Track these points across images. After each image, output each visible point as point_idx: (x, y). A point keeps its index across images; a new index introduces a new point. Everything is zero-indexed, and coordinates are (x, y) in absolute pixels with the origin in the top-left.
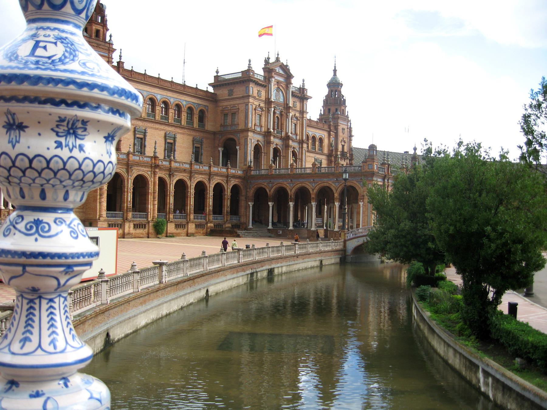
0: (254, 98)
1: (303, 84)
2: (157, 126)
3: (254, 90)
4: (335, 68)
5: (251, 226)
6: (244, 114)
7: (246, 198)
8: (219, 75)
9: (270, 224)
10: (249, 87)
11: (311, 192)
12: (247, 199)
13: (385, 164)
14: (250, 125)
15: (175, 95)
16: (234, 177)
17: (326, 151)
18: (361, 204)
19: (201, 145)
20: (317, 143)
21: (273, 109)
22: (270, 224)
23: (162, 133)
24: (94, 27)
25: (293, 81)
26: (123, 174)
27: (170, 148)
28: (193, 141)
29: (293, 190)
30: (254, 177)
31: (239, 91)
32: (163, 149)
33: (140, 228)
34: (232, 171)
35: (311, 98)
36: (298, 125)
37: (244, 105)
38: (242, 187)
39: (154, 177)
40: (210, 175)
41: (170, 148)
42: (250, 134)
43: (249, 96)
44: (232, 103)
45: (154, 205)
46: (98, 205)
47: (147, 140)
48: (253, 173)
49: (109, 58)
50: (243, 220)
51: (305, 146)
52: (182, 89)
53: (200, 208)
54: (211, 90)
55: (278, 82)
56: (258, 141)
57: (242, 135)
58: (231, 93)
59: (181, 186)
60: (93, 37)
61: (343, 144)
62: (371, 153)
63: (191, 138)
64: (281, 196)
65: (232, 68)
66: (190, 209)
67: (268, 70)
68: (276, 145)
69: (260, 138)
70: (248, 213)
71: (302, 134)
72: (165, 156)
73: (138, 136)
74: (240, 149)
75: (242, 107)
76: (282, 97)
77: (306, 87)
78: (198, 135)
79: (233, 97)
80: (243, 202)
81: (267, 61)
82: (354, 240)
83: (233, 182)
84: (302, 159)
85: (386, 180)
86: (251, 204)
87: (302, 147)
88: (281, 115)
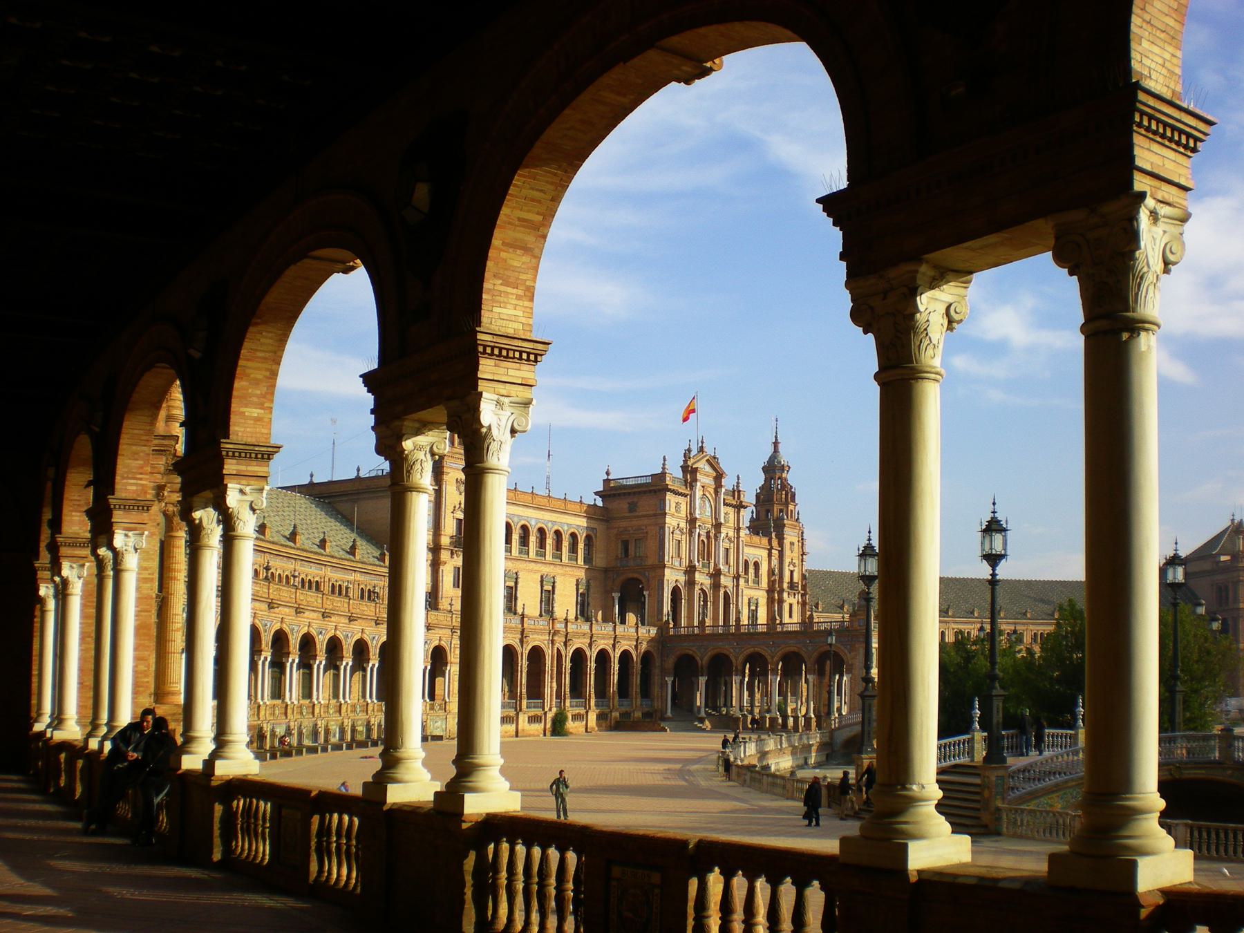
2: (532, 566)
5: (669, 714)
12: (664, 673)
27: (548, 599)
28: (577, 585)
41: (548, 599)
44: (635, 522)
50: (657, 704)
53: (601, 692)
54: (600, 503)
58: (632, 508)
59: (579, 656)
65: (633, 467)
76: (708, 509)
86: (669, 680)
87: (738, 586)
88: (708, 537)
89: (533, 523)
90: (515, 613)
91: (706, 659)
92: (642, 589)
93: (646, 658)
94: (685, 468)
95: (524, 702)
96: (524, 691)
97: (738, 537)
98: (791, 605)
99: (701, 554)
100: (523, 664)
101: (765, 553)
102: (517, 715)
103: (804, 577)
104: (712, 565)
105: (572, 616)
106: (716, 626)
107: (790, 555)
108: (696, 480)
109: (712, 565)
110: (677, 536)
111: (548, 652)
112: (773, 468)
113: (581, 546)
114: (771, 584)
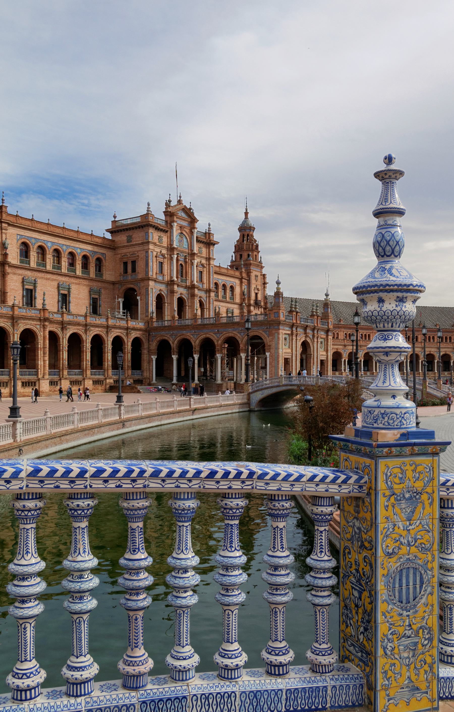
0: (155, 244)
2: (49, 276)
3: (154, 236)
4: (246, 211)
5: (154, 381)
6: (145, 262)
7: (149, 352)
8: (116, 219)
10: (148, 232)
11: (216, 343)
13: (293, 311)
14: (150, 273)
15: (68, 243)
17: (238, 299)
18: (268, 354)
19: (99, 296)
20: (228, 291)
21: (176, 256)
23: (55, 284)
25: (197, 225)
26: (8, 328)
27: (64, 299)
28: (90, 292)
29: (197, 342)
30: (156, 329)
31: (138, 236)
33: (29, 385)
34: (132, 324)
35: (218, 243)
36: (205, 272)
37: (144, 252)
38: (144, 340)
39: (44, 331)
40: (108, 328)
41: (64, 299)
42: (151, 283)
43: (148, 242)
44: (131, 250)
45: (44, 361)
47: (37, 291)
48: (155, 324)
51: (212, 294)
52: (76, 236)
54: (108, 236)
55: (181, 227)
56: (160, 290)
57: (142, 284)
58: (129, 239)
59: (75, 340)
61: (257, 292)
62: (277, 301)
64: (185, 348)
65: (129, 212)
66: (86, 364)
67: (169, 214)
68: (181, 294)
69: (163, 287)
70: (151, 368)
71: (209, 282)
73: (26, 287)
74: (141, 300)
75: (142, 255)
77: (212, 232)
78: (96, 285)
79: (132, 243)
80: (145, 356)
81: (168, 204)
82: (258, 393)
83: (134, 335)
84: (209, 309)
85: (294, 329)
86: (154, 358)
87: (209, 296)
88: (186, 262)
89: (49, 244)
91: (176, 342)
92: (136, 295)
101: (237, 282)
114: (243, 300)
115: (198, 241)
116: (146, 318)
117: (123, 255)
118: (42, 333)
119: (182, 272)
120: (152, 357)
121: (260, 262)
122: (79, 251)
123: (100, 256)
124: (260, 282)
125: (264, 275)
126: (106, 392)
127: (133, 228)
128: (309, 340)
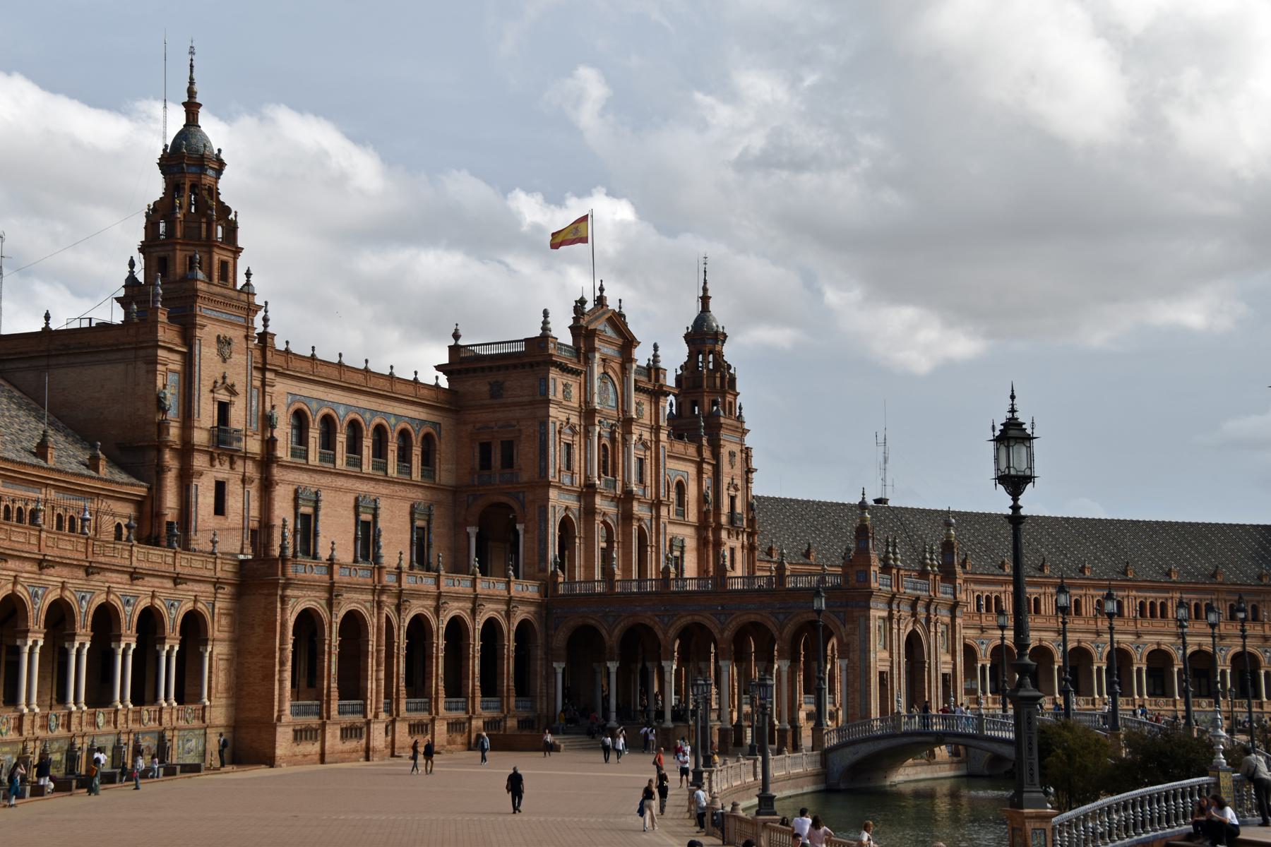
1: (655, 356)
2: (340, 482)
8: (461, 342)
9: (613, 715)
10: (546, 380)
12: (550, 656)
14: (551, 471)
16: (523, 601)
17: (692, 516)
22: (613, 715)
23: (350, 499)
24: (216, 258)
28: (412, 514)
32: (352, 536)
36: (648, 461)
38: (536, 625)
39: (379, 613)
42: (553, 494)
45: (378, 680)
46: (277, 687)
47: (321, 518)
49: (248, 328)
51: (664, 511)
54: (444, 382)
55: (604, 360)
56: (567, 508)
58: (497, 391)
60: (216, 281)
61: (732, 493)
63: (407, 507)
71: (657, 482)
72: (355, 556)
73: (303, 510)
74: (526, 531)
76: (612, 396)
77: (662, 365)
82: (847, 750)
83: (521, 613)
84: (658, 548)
85: (894, 606)
86: (559, 667)
87: (658, 517)
88: (613, 440)
89: (341, 411)
90: (315, 557)
93: (524, 625)
94: (574, 329)
95: (335, 705)
96: (334, 685)
97: (658, 441)
98: (732, 550)
99: (604, 468)
100: (333, 639)
101: (691, 469)
102: (323, 725)
103: (750, 507)
104: (619, 484)
105: (405, 565)
106: (627, 580)
107: (730, 473)
108: (593, 349)
109: (619, 484)
110: (567, 438)
111: (372, 622)
112: (704, 337)
113: (417, 451)
114: (703, 515)
115: (638, 389)
116: (541, 575)
117: (478, 425)
118: (375, 620)
119: (605, 462)
120: (555, 665)
121: (740, 418)
122: (393, 421)
123: (431, 430)
124: (738, 470)
125: (747, 452)
126: (469, 749)
127: (507, 367)
128: (920, 630)
